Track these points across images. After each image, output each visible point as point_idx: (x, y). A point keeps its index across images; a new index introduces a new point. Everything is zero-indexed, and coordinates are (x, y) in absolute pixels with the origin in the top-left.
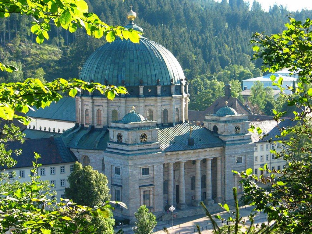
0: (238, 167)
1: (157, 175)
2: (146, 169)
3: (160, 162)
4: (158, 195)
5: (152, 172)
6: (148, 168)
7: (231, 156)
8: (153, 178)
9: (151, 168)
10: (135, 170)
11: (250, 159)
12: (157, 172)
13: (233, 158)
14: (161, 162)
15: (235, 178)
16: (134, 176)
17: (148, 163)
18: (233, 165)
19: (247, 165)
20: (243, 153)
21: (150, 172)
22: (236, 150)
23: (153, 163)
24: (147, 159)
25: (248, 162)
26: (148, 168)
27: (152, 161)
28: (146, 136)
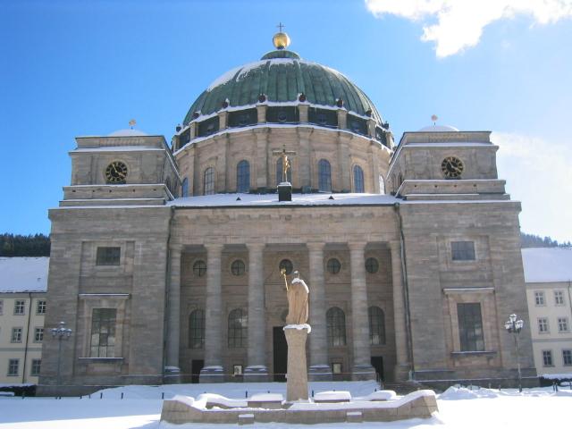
0: (461, 272)
1: (142, 268)
2: (109, 250)
3: (155, 233)
4: (142, 326)
5: (130, 261)
6: (118, 249)
7: (427, 235)
8: (132, 277)
9: (123, 250)
10: (69, 249)
11: (504, 248)
13: (435, 243)
14: (160, 234)
15: (450, 305)
16: (66, 264)
17: (115, 233)
18: (435, 261)
20: (472, 226)
21: (122, 259)
23: (132, 235)
25: (495, 257)
26: (118, 249)
28: (126, 169)
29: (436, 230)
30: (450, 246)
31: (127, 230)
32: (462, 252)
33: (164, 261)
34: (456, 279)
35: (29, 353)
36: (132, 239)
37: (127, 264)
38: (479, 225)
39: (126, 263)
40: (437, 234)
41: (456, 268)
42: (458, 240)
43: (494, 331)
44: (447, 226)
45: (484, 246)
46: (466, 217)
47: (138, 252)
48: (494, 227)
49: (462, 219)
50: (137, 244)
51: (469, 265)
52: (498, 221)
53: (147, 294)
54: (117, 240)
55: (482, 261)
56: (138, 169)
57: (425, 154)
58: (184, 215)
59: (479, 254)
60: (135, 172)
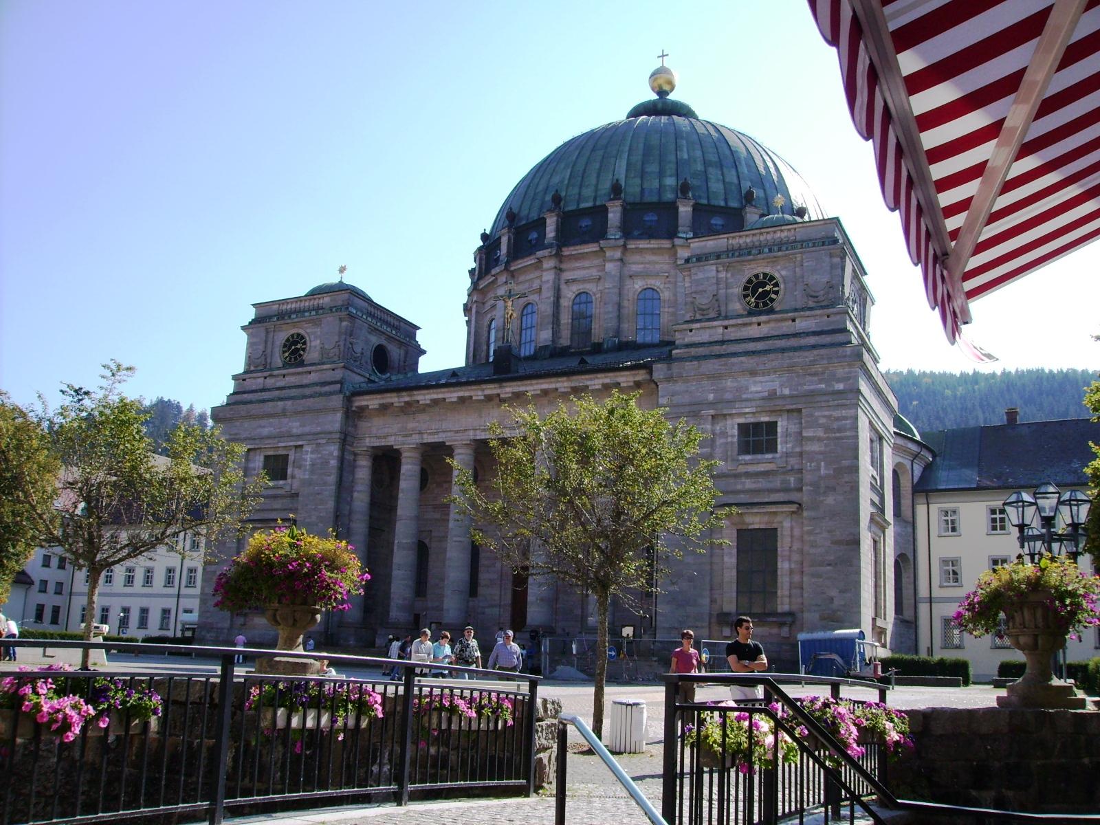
0: (747, 475)
1: (309, 483)
9: (291, 458)
11: (827, 429)
12: (312, 472)
14: (331, 433)
19: (809, 466)
20: (772, 395)
22: (729, 383)
23: (299, 437)
24: (274, 421)
27: (295, 426)
29: (711, 404)
30: (735, 432)
31: (295, 431)
32: (757, 438)
33: (335, 471)
34: (739, 487)
35: (181, 600)
36: (300, 443)
37: (298, 475)
38: (787, 392)
39: (293, 477)
40: (712, 412)
41: (742, 469)
42: (751, 420)
43: (797, 578)
44: (728, 396)
45: (793, 428)
46: (767, 378)
47: (306, 460)
48: (812, 394)
49: (755, 383)
50: (305, 448)
51: (764, 462)
52: (820, 382)
53: (314, 519)
54: (283, 444)
55: (787, 455)
56: (318, 341)
57: (714, 273)
58: (364, 403)
59: (781, 444)
60: (315, 347)
